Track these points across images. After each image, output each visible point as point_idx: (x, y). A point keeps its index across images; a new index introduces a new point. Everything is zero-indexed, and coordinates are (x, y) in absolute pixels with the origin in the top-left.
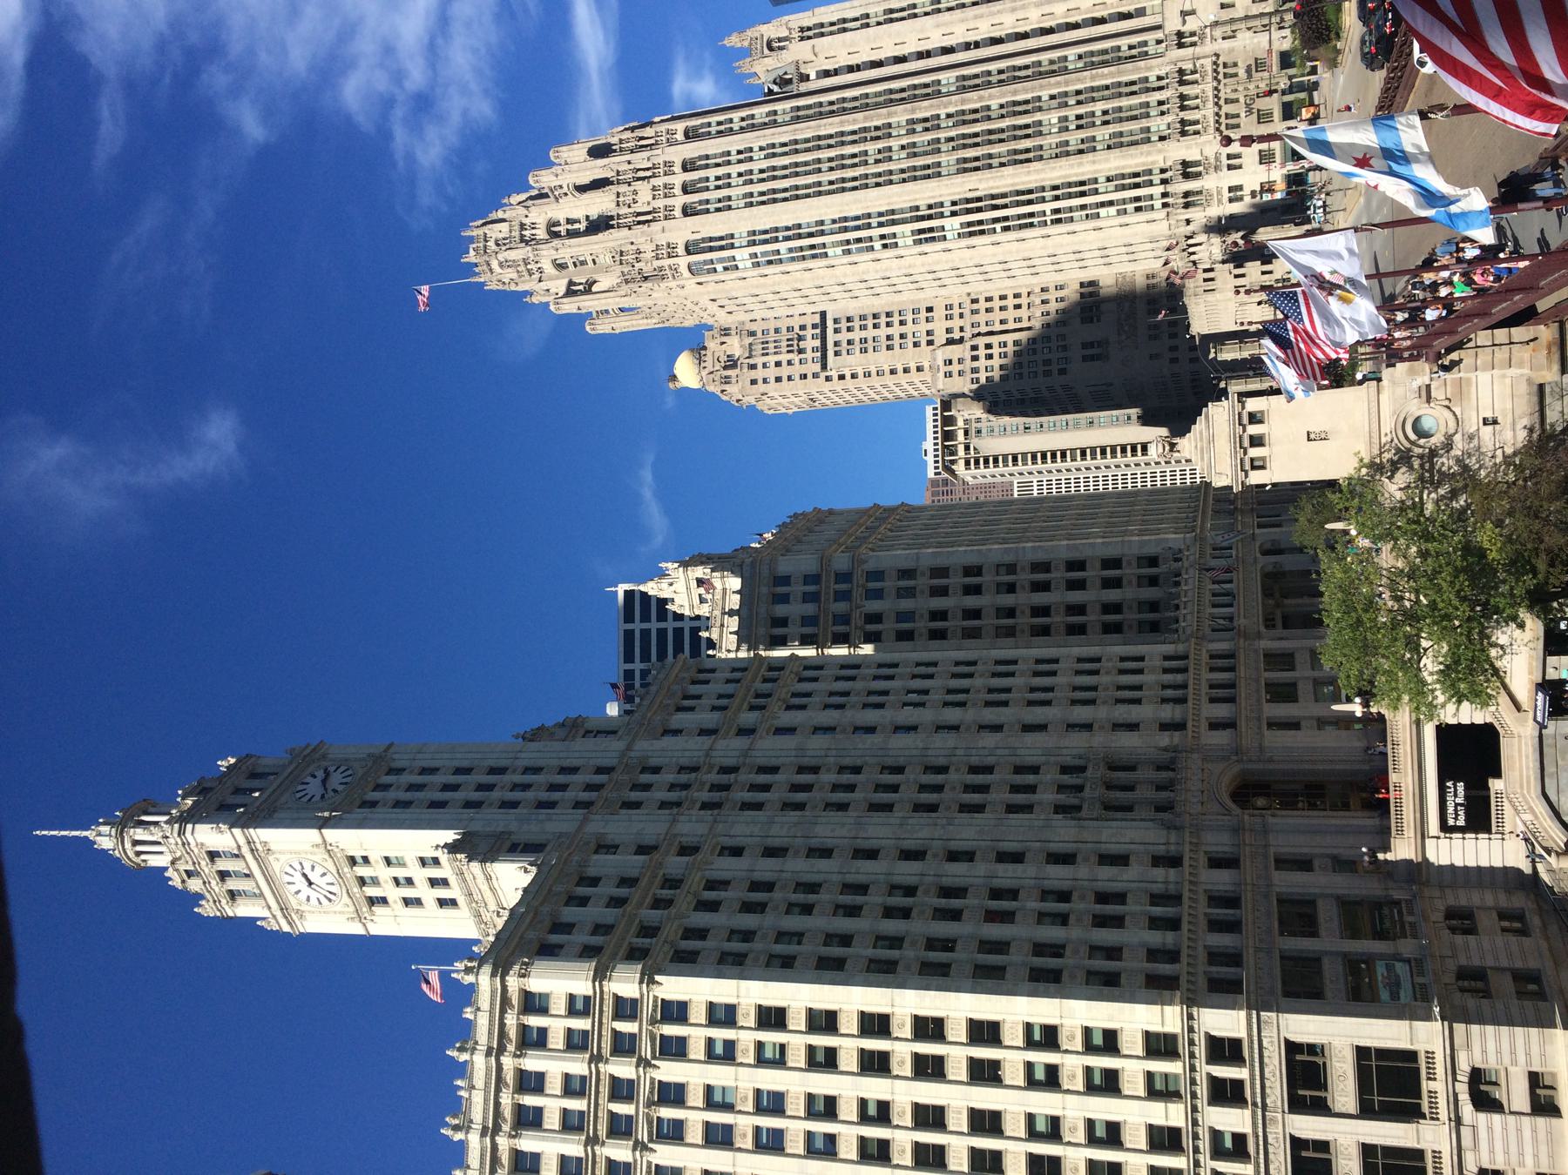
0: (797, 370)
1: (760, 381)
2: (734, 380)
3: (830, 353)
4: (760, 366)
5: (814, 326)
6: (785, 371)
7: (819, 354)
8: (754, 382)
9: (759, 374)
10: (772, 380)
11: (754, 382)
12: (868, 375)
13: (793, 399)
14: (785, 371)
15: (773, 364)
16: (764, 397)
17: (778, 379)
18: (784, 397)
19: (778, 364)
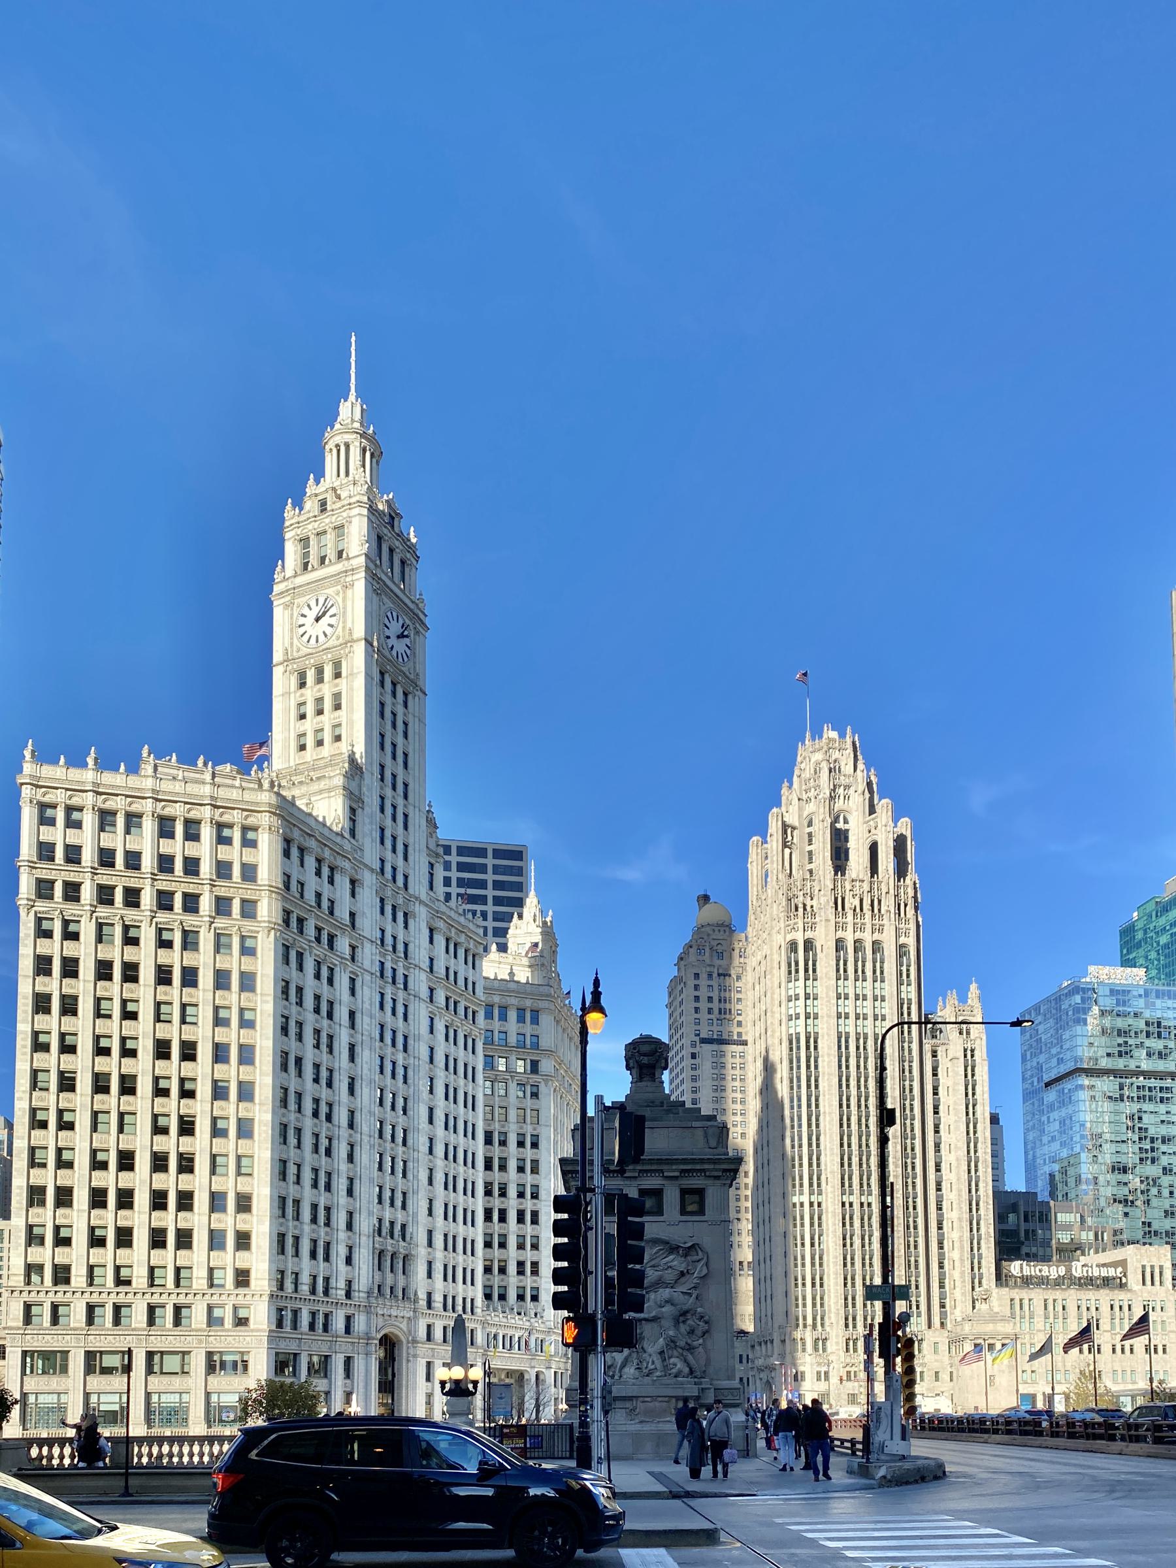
0: (704, 1016)
1: (697, 982)
2: (700, 958)
3: (715, 1047)
4: (710, 983)
5: (740, 1034)
6: (704, 1005)
7: (715, 1037)
8: (697, 976)
9: (703, 982)
10: (697, 993)
11: (697, 976)
12: (694, 1079)
13: (679, 1010)
14: (704, 1005)
15: (711, 994)
16: (682, 985)
17: (697, 999)
18: (681, 1003)
19: (710, 999)
